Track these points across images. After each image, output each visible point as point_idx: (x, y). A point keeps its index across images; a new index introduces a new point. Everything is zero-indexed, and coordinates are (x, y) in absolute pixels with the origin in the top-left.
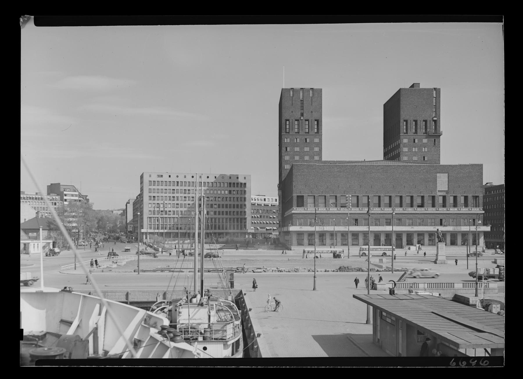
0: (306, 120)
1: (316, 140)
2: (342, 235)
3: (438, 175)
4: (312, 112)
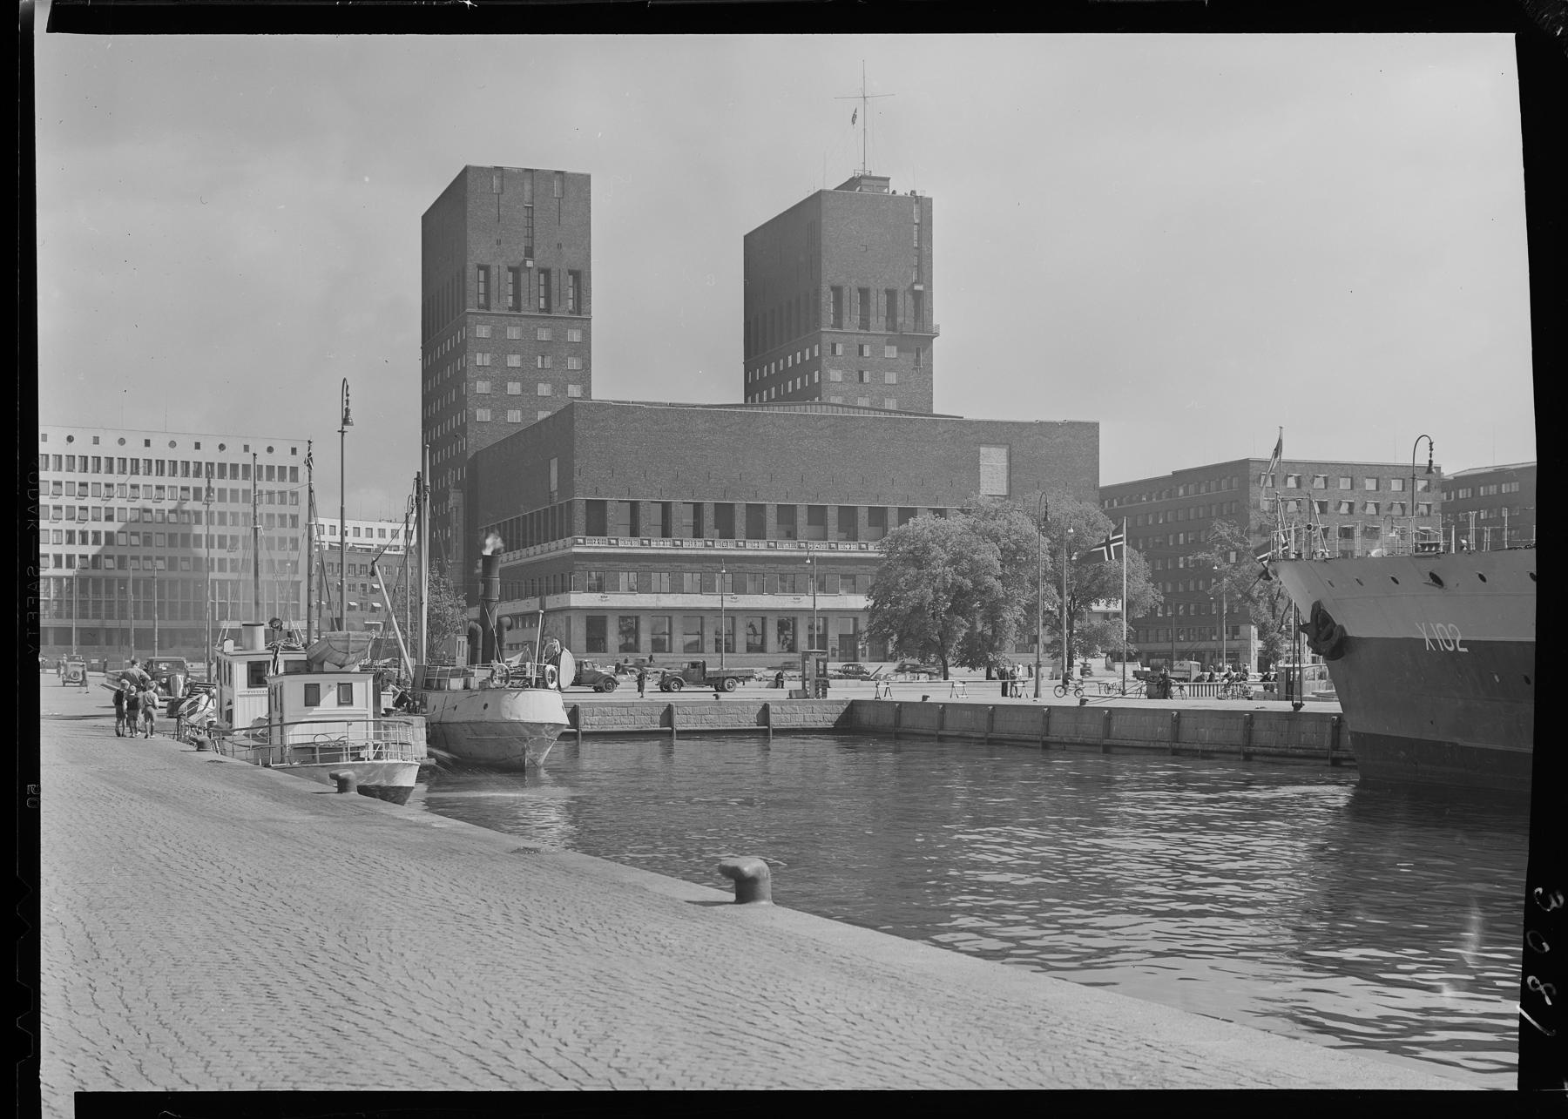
0: (542, 271)
1: (575, 336)
2: (783, 626)
3: (983, 450)
4: (559, 246)
